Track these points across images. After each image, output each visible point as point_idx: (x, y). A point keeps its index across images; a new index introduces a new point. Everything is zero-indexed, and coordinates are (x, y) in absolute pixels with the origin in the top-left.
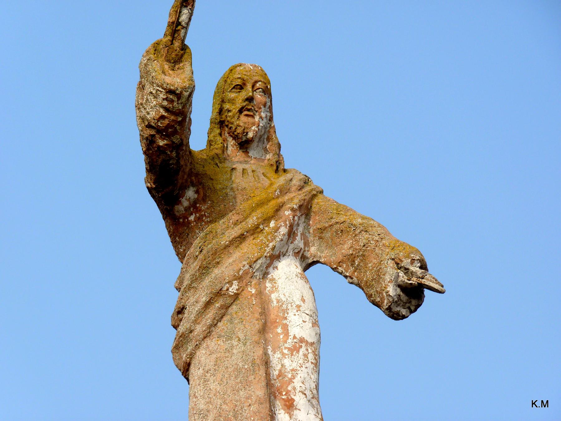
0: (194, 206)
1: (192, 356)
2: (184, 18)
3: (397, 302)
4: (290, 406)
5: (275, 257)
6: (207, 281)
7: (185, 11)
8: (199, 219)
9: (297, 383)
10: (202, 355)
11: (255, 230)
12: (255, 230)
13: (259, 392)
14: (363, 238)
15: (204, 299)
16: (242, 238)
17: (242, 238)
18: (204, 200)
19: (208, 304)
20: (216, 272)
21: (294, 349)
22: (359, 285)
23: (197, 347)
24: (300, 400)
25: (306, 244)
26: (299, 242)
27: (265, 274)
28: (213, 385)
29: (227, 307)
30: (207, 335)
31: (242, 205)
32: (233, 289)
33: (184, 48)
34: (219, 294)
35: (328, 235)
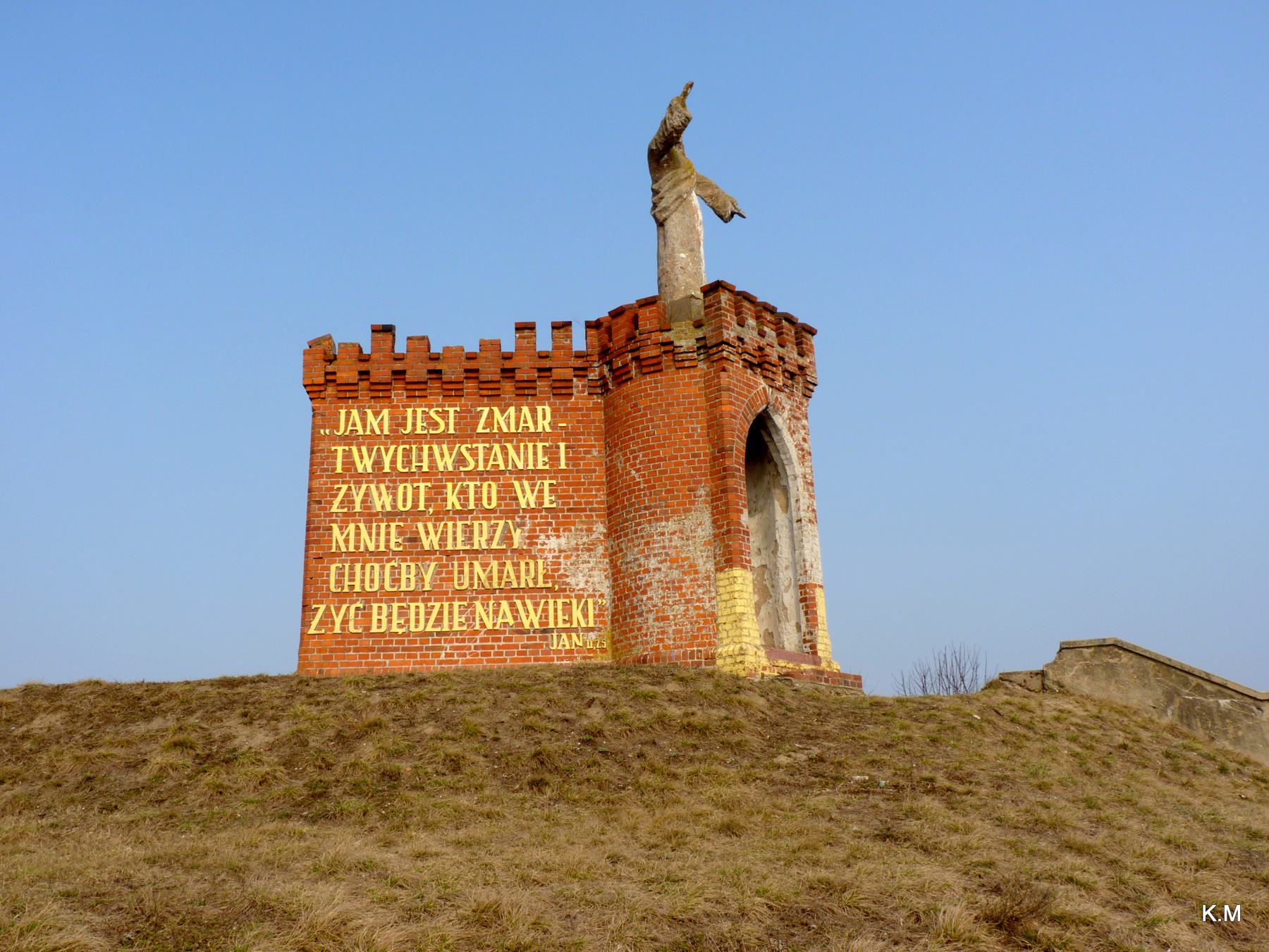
0: (667, 160)
1: (669, 216)
6: (675, 190)
8: (668, 166)
10: (673, 216)
14: (716, 191)
15: (675, 197)
18: (671, 160)
19: (676, 199)
20: (678, 188)
22: (711, 207)
23: (672, 214)
28: (679, 229)
29: (682, 202)
30: (675, 210)
32: (685, 196)
35: (701, 185)
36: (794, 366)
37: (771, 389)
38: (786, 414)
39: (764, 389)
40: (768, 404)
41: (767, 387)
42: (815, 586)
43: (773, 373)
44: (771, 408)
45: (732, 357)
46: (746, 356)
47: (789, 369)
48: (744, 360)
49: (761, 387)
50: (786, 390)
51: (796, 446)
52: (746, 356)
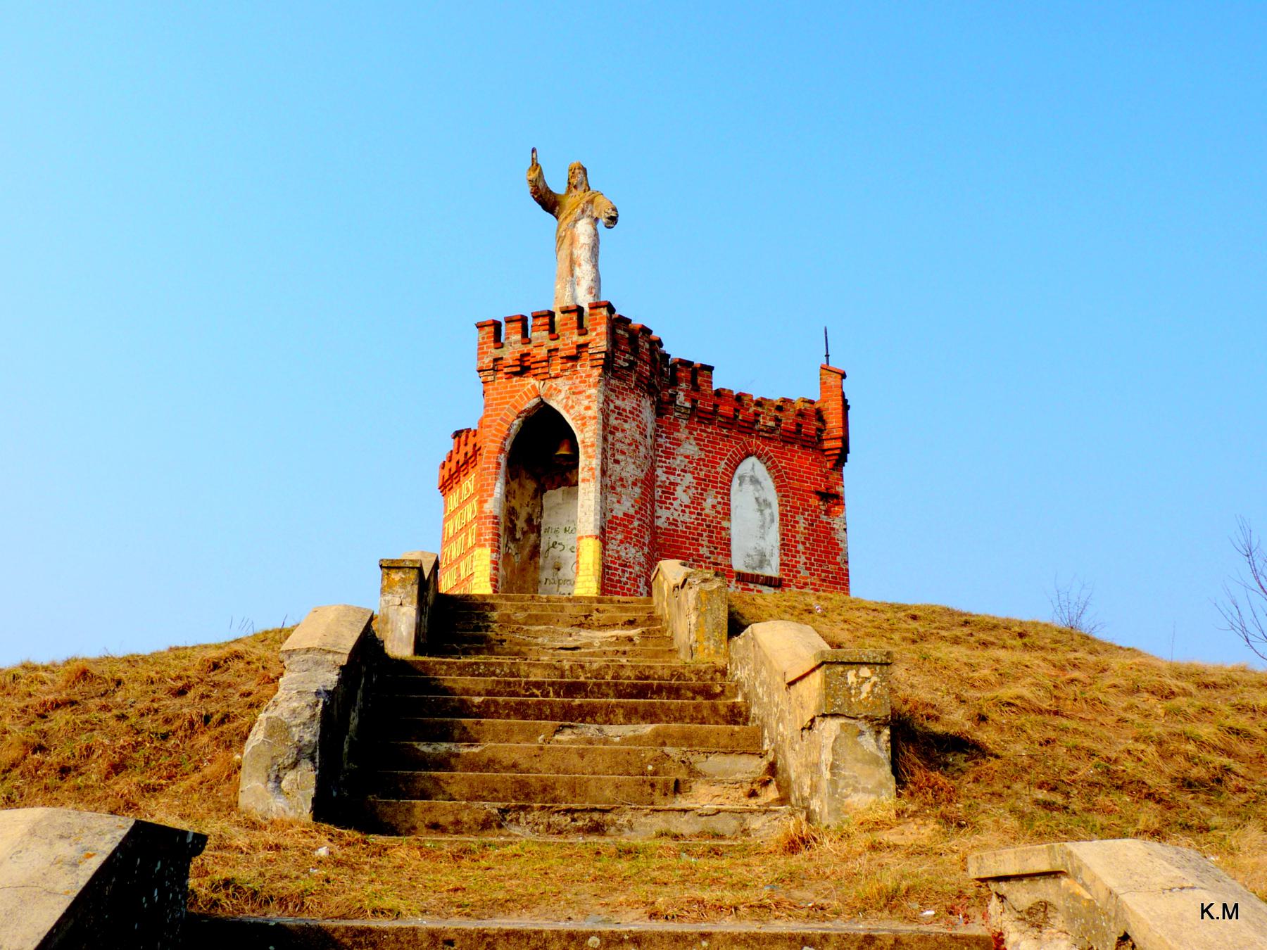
2: (534, 156)
3: (608, 223)
4: (580, 265)
5: (576, 221)
7: (534, 154)
9: (582, 258)
11: (570, 214)
12: (570, 214)
13: (567, 263)
16: (566, 218)
17: (566, 218)
21: (582, 247)
24: (583, 262)
25: (592, 213)
26: (588, 213)
27: (574, 227)
31: (567, 208)
33: (537, 165)
34: (560, 237)
36: (572, 348)
37: (542, 382)
38: (562, 396)
39: (534, 387)
40: (539, 396)
41: (537, 383)
42: (581, 538)
43: (542, 367)
44: (543, 398)
45: (490, 378)
46: (506, 370)
47: (563, 355)
48: (506, 373)
49: (529, 386)
50: (567, 373)
51: (573, 419)
52: (506, 370)
